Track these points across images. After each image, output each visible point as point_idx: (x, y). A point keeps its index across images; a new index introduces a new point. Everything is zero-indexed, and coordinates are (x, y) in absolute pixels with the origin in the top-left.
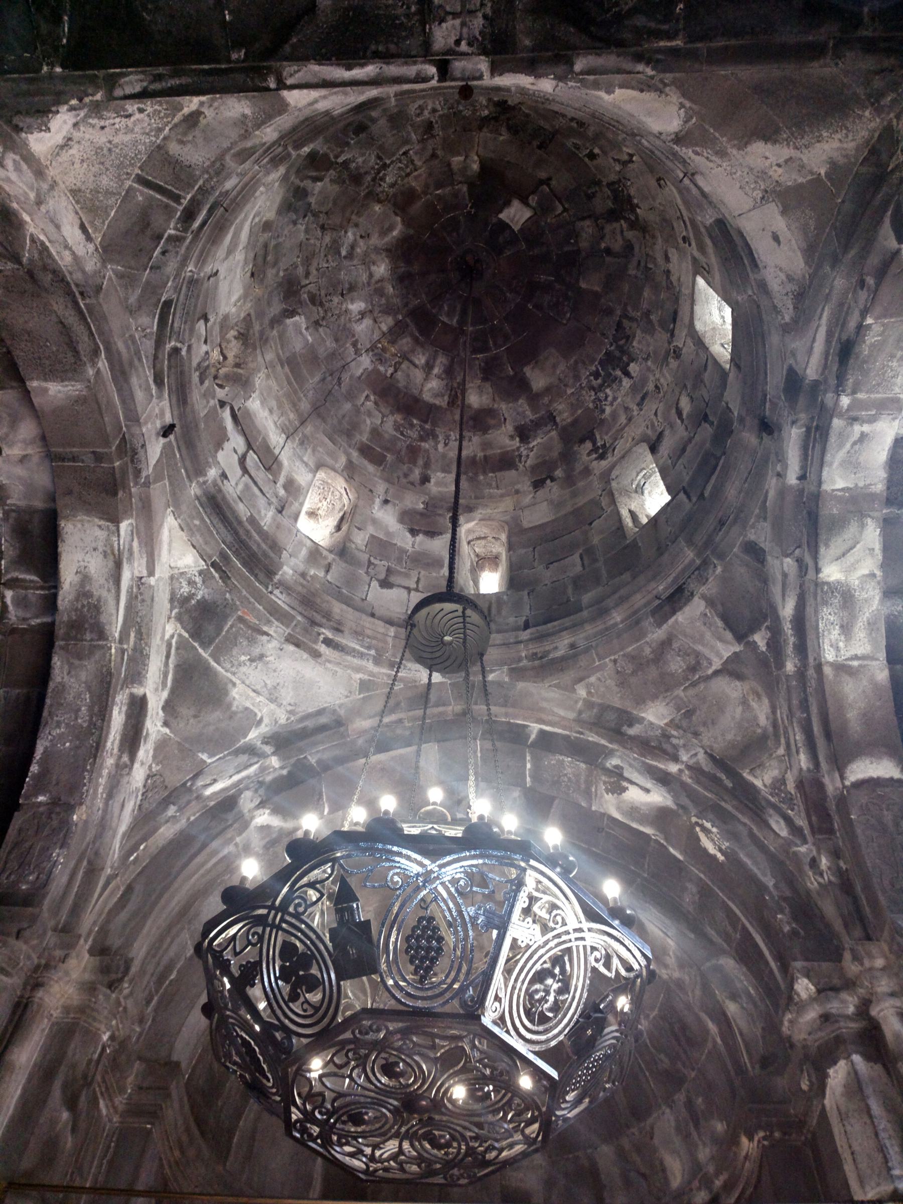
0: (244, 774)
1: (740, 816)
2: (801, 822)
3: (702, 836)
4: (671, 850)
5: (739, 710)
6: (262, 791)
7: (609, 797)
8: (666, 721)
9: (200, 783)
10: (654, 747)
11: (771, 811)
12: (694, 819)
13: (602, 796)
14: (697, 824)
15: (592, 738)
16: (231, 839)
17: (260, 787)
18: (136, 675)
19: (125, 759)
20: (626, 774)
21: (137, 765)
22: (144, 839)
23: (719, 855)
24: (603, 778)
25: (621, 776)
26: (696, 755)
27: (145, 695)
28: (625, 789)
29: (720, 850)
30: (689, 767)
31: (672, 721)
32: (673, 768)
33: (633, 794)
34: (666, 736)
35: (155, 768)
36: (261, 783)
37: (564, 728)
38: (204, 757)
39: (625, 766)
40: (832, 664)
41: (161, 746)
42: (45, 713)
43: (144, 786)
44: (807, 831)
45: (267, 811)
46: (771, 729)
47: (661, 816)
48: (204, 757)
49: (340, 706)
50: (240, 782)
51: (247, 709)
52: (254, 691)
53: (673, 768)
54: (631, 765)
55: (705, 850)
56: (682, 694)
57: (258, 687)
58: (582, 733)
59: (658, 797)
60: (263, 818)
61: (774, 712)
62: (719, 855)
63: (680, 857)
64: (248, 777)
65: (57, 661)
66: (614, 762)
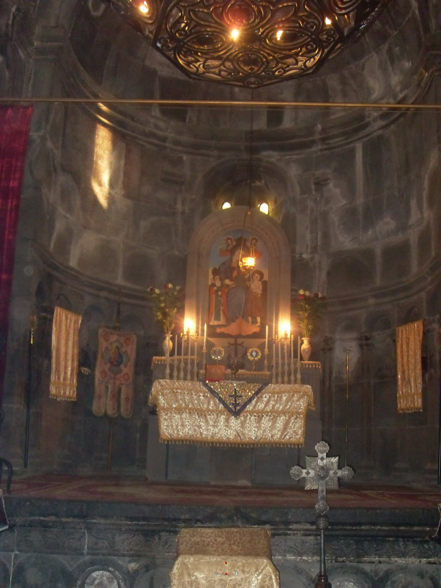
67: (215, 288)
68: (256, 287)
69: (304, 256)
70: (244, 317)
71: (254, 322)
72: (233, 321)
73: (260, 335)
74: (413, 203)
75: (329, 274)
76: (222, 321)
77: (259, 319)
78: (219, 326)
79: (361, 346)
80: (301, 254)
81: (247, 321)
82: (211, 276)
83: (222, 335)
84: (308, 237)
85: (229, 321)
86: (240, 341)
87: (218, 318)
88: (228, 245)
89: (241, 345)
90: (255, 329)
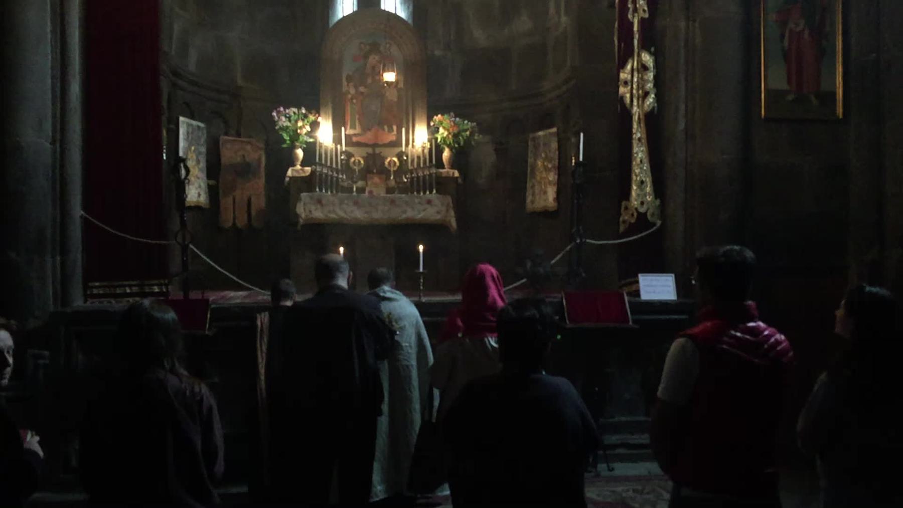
67: (350, 96)
68: (392, 95)
70: (381, 124)
71: (391, 130)
72: (369, 130)
73: (397, 143)
76: (358, 130)
77: (395, 128)
78: (355, 135)
81: (384, 130)
83: (358, 144)
85: (365, 129)
86: (378, 150)
87: (353, 127)
90: (392, 137)
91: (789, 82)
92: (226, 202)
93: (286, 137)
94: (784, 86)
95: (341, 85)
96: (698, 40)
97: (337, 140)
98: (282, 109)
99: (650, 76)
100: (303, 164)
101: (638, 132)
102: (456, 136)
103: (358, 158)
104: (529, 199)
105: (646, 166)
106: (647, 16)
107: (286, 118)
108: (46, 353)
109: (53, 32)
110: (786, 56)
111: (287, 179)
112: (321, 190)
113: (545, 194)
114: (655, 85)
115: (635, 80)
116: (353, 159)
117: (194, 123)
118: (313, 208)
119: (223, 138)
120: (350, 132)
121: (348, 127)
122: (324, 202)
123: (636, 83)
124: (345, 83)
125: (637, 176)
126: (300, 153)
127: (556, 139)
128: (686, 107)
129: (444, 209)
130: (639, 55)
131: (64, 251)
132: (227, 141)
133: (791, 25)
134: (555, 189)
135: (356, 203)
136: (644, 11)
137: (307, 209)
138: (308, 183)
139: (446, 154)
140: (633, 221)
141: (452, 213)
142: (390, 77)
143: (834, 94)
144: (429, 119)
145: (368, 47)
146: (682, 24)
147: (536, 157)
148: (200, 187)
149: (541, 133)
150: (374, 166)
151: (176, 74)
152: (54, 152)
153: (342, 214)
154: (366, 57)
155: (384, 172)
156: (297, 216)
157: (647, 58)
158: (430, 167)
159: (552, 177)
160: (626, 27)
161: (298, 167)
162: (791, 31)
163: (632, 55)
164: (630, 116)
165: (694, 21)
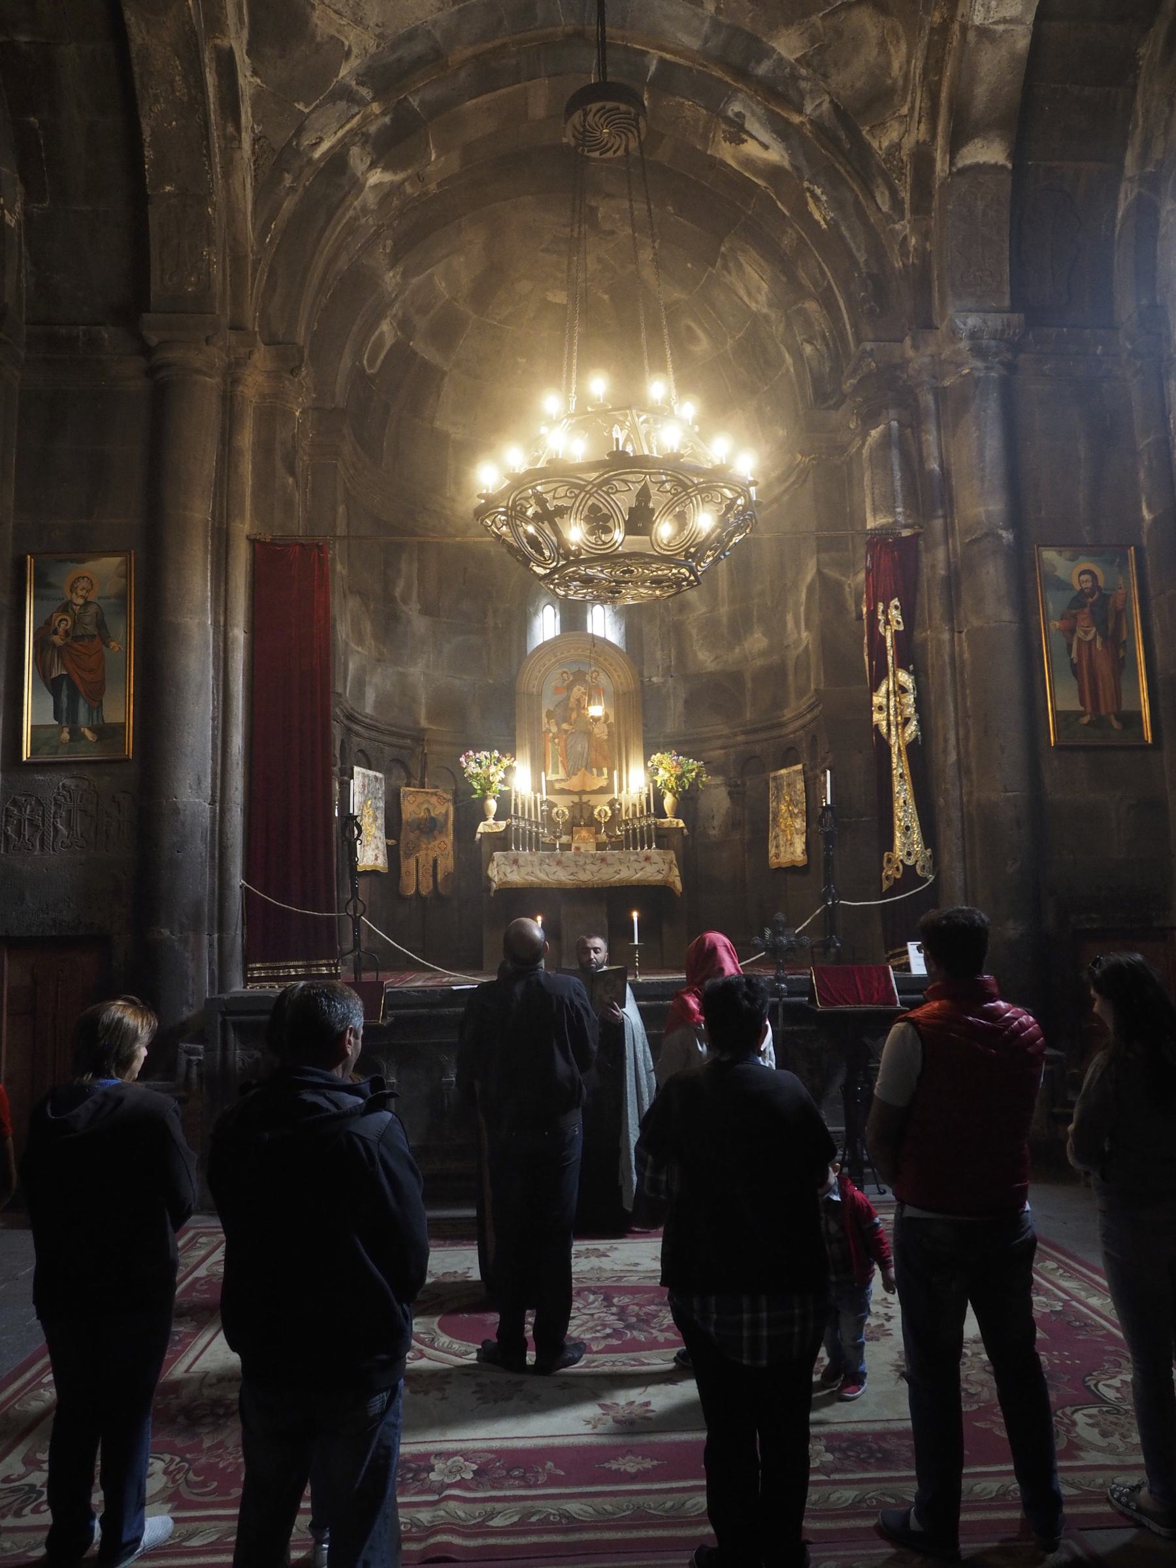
0: (347, 127)
1: (851, 182)
2: (906, 195)
3: (810, 200)
4: (779, 204)
5: (875, 52)
6: (369, 148)
7: (726, 145)
8: (798, 55)
9: (306, 142)
10: (777, 94)
11: (880, 181)
12: (806, 184)
13: (719, 143)
14: (808, 189)
15: (718, 73)
16: (352, 203)
17: (366, 142)
18: (216, 24)
19: (230, 129)
20: (747, 126)
21: (243, 134)
22: (271, 218)
23: (822, 223)
24: (723, 126)
25: (742, 128)
26: (820, 105)
27: (231, 48)
28: (743, 141)
29: (825, 219)
30: (812, 122)
31: (804, 56)
32: (796, 119)
33: (751, 148)
34: (795, 77)
35: (258, 129)
36: (366, 135)
37: (686, 58)
38: (300, 106)
39: (748, 115)
40: (977, 28)
41: (257, 100)
42: (138, 85)
43: (253, 153)
44: (907, 206)
45: (379, 170)
46: (901, 82)
47: (774, 173)
48: (300, 106)
49: (435, 23)
50: (344, 136)
51: (332, 37)
52: (336, 12)
53: (796, 119)
54: (753, 113)
55: (810, 214)
56: (819, 23)
57: (339, 6)
58: (705, 66)
59: (776, 155)
60: (376, 177)
61: (909, 62)
62: (822, 223)
63: (787, 213)
64: (351, 130)
65: (130, 16)
66: (735, 107)
68: (601, 732)
69: (654, 679)
70: (588, 767)
71: (600, 774)
74: (789, 618)
75: (686, 702)
76: (562, 775)
77: (605, 770)
79: (730, 794)
80: (650, 678)
81: (592, 773)
82: (545, 720)
83: (562, 792)
84: (659, 655)
85: (570, 774)
86: (585, 798)
87: (556, 771)
88: (564, 680)
89: (586, 803)
90: (602, 782)
91: (1082, 702)
92: (408, 865)
93: (476, 785)
94: (1076, 706)
95: (540, 723)
96: (966, 655)
97: (537, 789)
98: (471, 753)
99: (910, 699)
100: (496, 818)
101: (899, 766)
102: (679, 778)
103: (562, 806)
104: (772, 851)
105: (912, 808)
106: (901, 628)
107: (474, 764)
108: (201, 1047)
109: (215, 678)
110: (1075, 670)
111: (478, 836)
112: (517, 848)
113: (790, 845)
114: (917, 710)
115: (892, 703)
116: (555, 810)
117: (371, 773)
118: (509, 870)
119: (404, 789)
120: (552, 777)
121: (550, 771)
122: (521, 862)
123: (892, 707)
124: (545, 720)
125: (900, 820)
126: (492, 805)
127: (802, 777)
128: (957, 734)
129: (666, 867)
130: (895, 675)
131: (222, 924)
132: (411, 793)
133: (1080, 633)
134: (804, 839)
135: (559, 863)
136: (898, 622)
137: (503, 871)
138: (502, 841)
139: (669, 801)
140: (898, 876)
141: (676, 872)
142: (596, 710)
143: (1140, 713)
144: (647, 758)
145: (571, 678)
146: (946, 636)
147: (778, 799)
148: (377, 848)
149: (783, 771)
150: (581, 817)
151: (350, 717)
152: (213, 811)
153: (543, 876)
154: (569, 688)
155: (592, 823)
156: (489, 880)
157: (905, 678)
158: (648, 816)
159: (800, 824)
160: (877, 644)
161: (491, 821)
162: (1079, 639)
163: (887, 675)
164: (889, 748)
165: (960, 632)
